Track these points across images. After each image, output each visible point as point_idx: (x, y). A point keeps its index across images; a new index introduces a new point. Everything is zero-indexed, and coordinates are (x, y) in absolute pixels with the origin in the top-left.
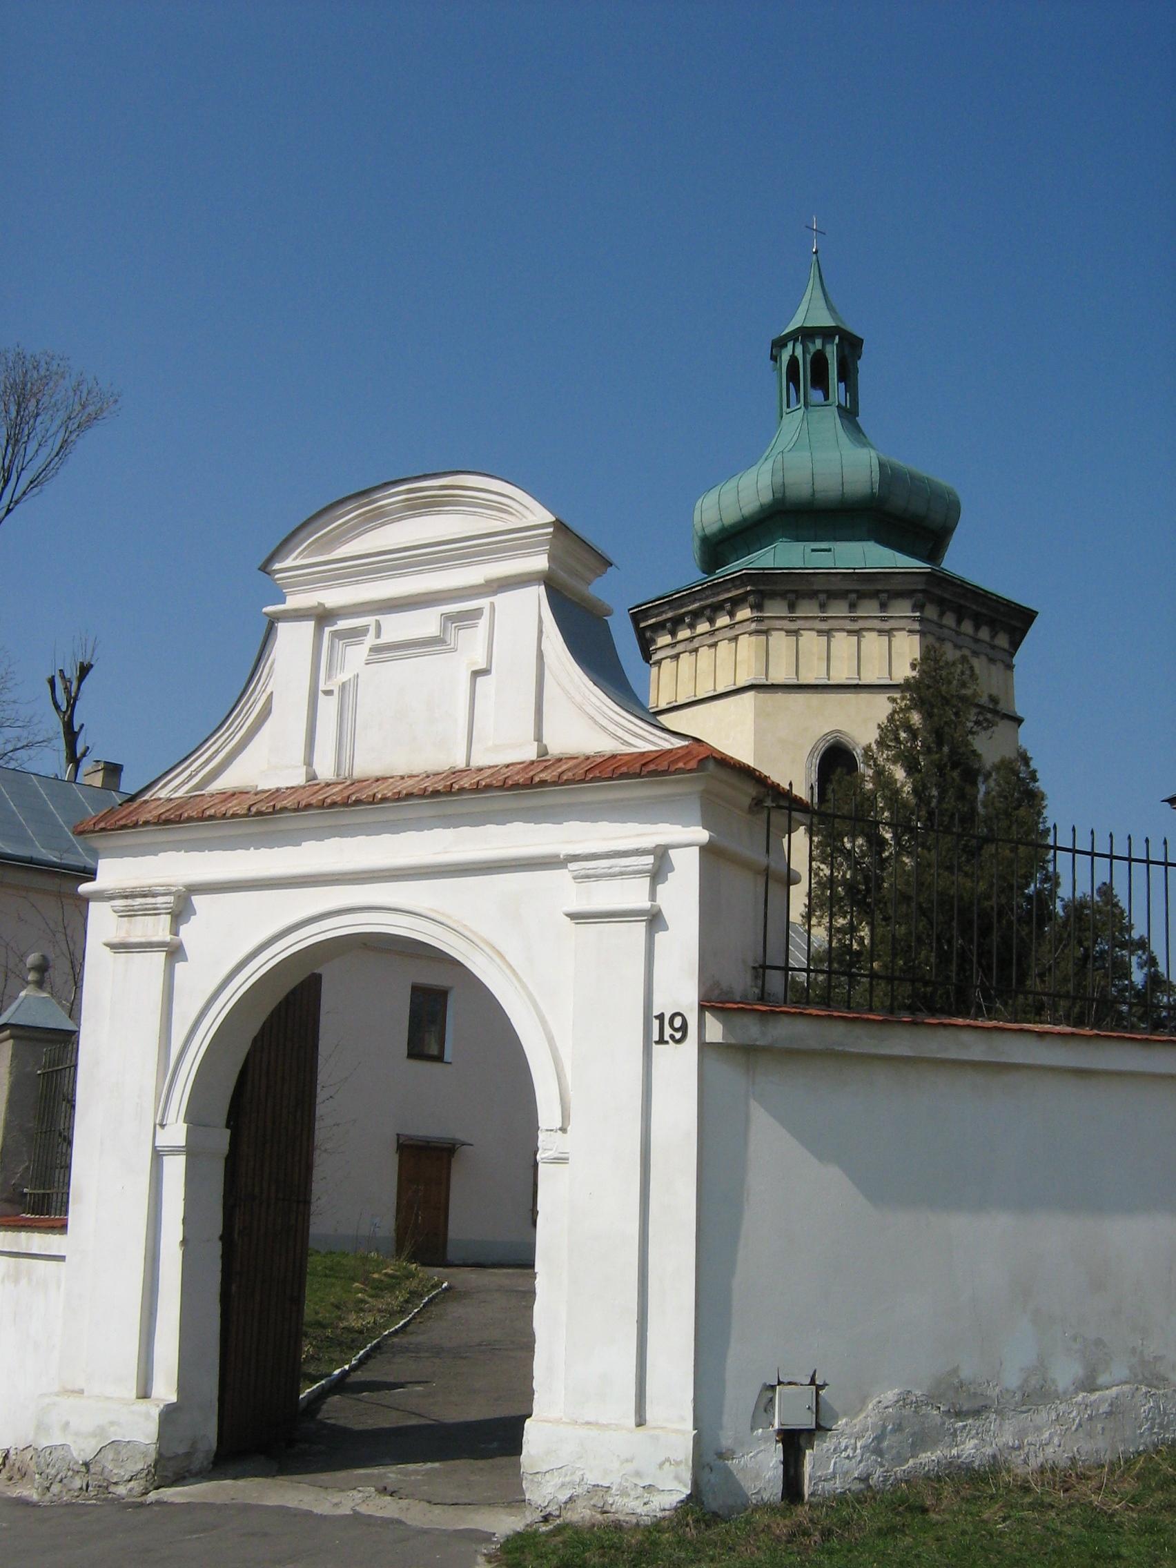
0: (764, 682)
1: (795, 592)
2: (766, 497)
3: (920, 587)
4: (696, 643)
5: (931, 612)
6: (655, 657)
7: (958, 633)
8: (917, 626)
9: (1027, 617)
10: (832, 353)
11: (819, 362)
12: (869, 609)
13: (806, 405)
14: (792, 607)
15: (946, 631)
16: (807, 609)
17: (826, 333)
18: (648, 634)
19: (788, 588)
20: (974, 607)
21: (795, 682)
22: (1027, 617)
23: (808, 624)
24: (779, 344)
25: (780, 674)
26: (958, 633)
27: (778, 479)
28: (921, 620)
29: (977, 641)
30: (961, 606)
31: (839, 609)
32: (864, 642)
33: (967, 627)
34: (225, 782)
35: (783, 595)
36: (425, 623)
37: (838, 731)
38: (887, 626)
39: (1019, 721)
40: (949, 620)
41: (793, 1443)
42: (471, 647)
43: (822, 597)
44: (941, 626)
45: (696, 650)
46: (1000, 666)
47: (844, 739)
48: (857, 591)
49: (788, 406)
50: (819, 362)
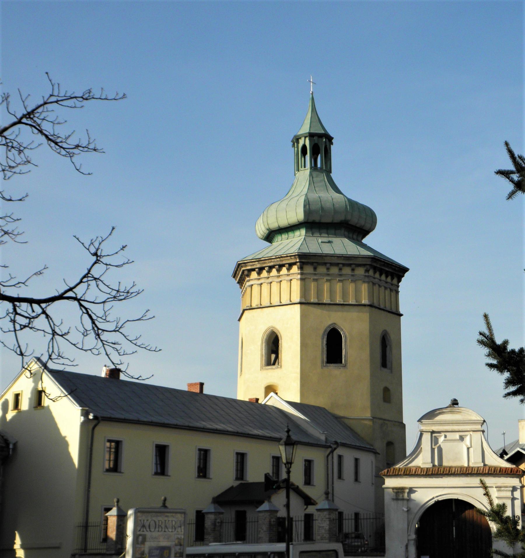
1: (317, 263)
4: (270, 280)
5: (371, 273)
7: (380, 280)
9: (406, 270)
15: (376, 280)
18: (246, 273)
19: (315, 261)
20: (387, 269)
22: (405, 270)
26: (380, 280)
29: (386, 282)
30: (382, 269)
33: (383, 277)
35: (312, 264)
37: (335, 324)
39: (402, 315)
43: (328, 265)
44: (374, 278)
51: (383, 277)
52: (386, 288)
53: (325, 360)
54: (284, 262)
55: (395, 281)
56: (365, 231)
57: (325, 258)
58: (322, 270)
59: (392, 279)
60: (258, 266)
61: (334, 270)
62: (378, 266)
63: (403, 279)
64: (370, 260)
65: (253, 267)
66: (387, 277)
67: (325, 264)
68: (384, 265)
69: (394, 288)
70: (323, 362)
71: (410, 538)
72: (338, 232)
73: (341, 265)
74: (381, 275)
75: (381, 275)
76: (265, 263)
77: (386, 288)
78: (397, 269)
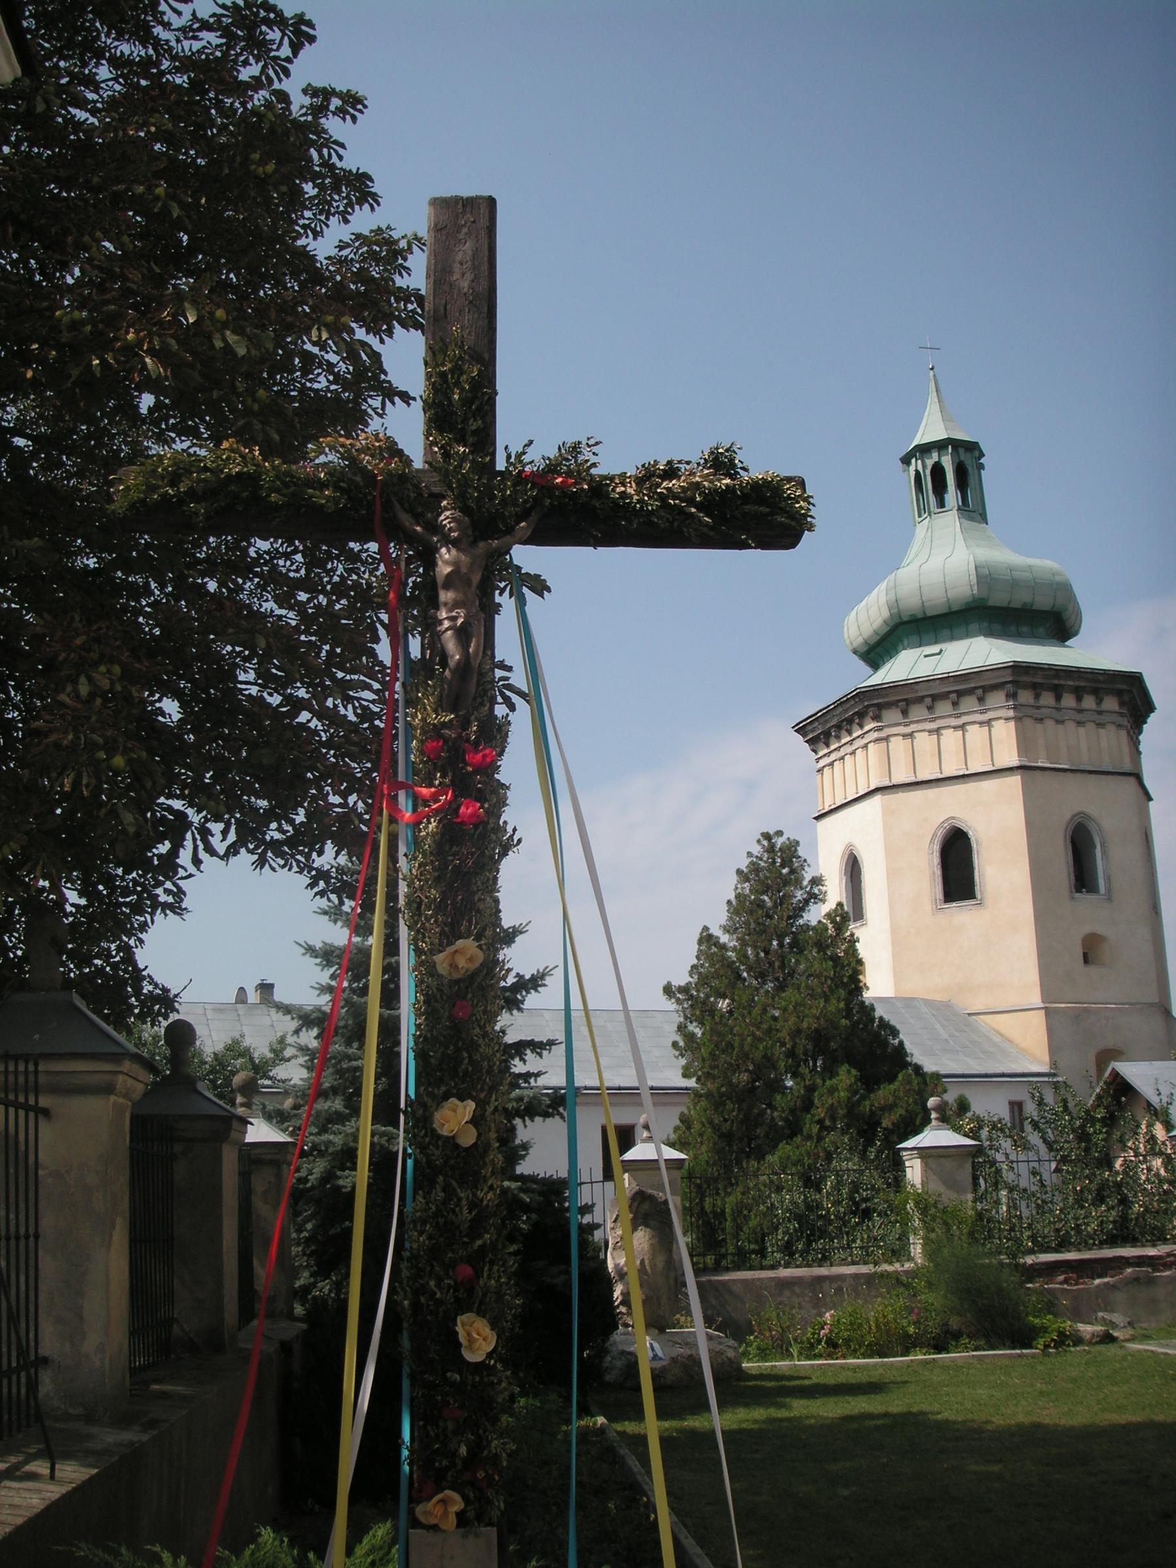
0: (887, 783)
2: (886, 614)
5: (1025, 697)
7: (1058, 709)
8: (1011, 713)
11: (938, 472)
13: (930, 514)
14: (905, 713)
15: (1044, 710)
17: (940, 446)
20: (1070, 683)
21: (912, 779)
27: (892, 597)
28: (1015, 708)
32: (967, 735)
37: (953, 818)
49: (920, 516)
50: (938, 472)
51: (1068, 701)
53: (940, 895)
57: (917, 687)
58: (918, 712)
61: (944, 707)
64: (1009, 671)
67: (920, 700)
72: (974, 626)
76: (826, 722)
78: (1101, 678)
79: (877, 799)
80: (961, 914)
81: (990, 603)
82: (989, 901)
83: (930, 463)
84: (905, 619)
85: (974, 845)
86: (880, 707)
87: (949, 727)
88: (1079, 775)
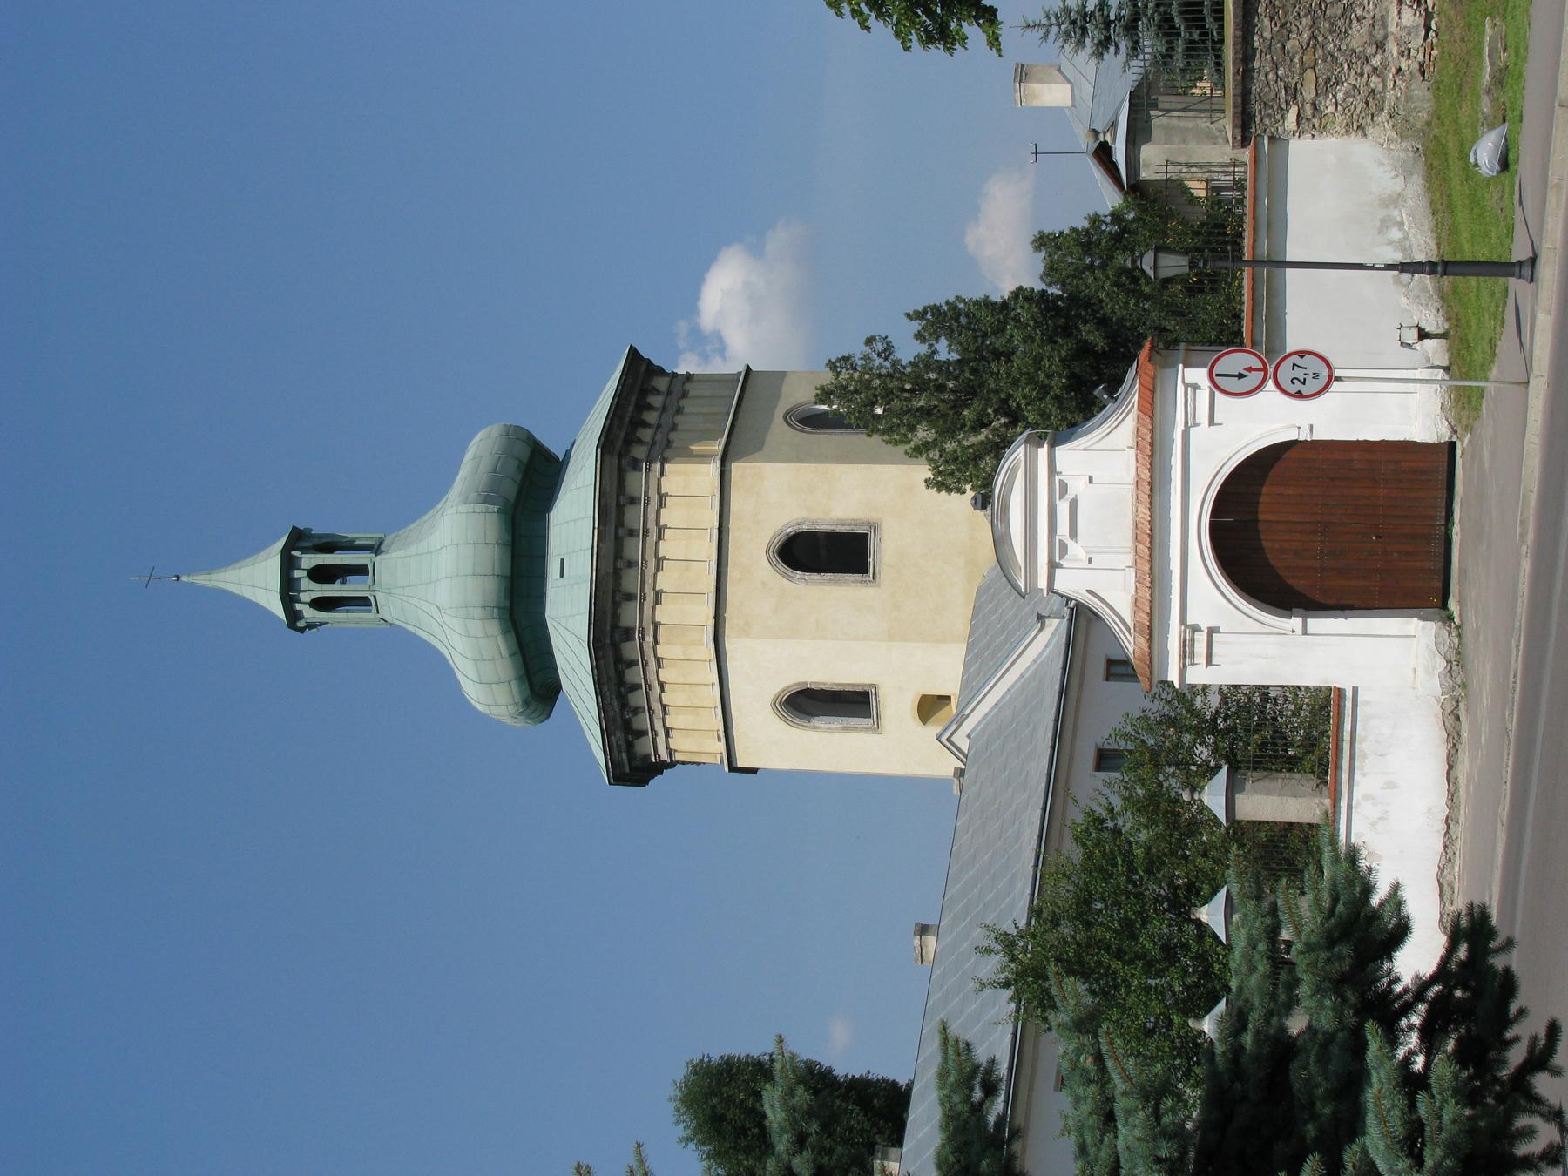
2: (494, 628)
3: (615, 461)
4: (656, 706)
5: (639, 452)
6: (665, 756)
7: (659, 426)
8: (657, 467)
9: (634, 356)
10: (310, 560)
11: (321, 574)
12: (634, 517)
15: (658, 437)
16: (631, 581)
17: (288, 564)
22: (634, 356)
23: (649, 580)
24: (293, 616)
25: (704, 612)
26: (659, 426)
28: (650, 461)
29: (664, 409)
31: (633, 548)
33: (652, 417)
34: (1126, 612)
35: (616, 605)
36: (1063, 508)
37: (768, 549)
38: (654, 498)
39: (748, 369)
40: (646, 434)
41: (1423, 335)
42: (1077, 487)
43: (620, 564)
44: (654, 443)
45: (664, 707)
46: (688, 386)
47: (777, 544)
48: (617, 528)
50: (321, 574)
51: (652, 417)
52: (679, 411)
53: (858, 577)
54: (612, 673)
55: (661, 383)
56: (533, 454)
57: (602, 573)
59: (656, 392)
60: (619, 734)
62: (622, 435)
63: (656, 362)
64: (607, 457)
65: (624, 747)
66: (650, 408)
67: (617, 574)
68: (621, 418)
69: (677, 388)
70: (867, 730)
71: (1299, 629)
73: (621, 532)
74: (645, 425)
75: (645, 425)
76: (614, 720)
77: (679, 411)
78: (630, 381)
79: (731, 645)
80: (884, 553)
81: (512, 499)
82: (873, 516)
83: (305, 583)
84: (507, 603)
85: (805, 528)
86: (615, 626)
87: (657, 544)
88: (740, 415)
